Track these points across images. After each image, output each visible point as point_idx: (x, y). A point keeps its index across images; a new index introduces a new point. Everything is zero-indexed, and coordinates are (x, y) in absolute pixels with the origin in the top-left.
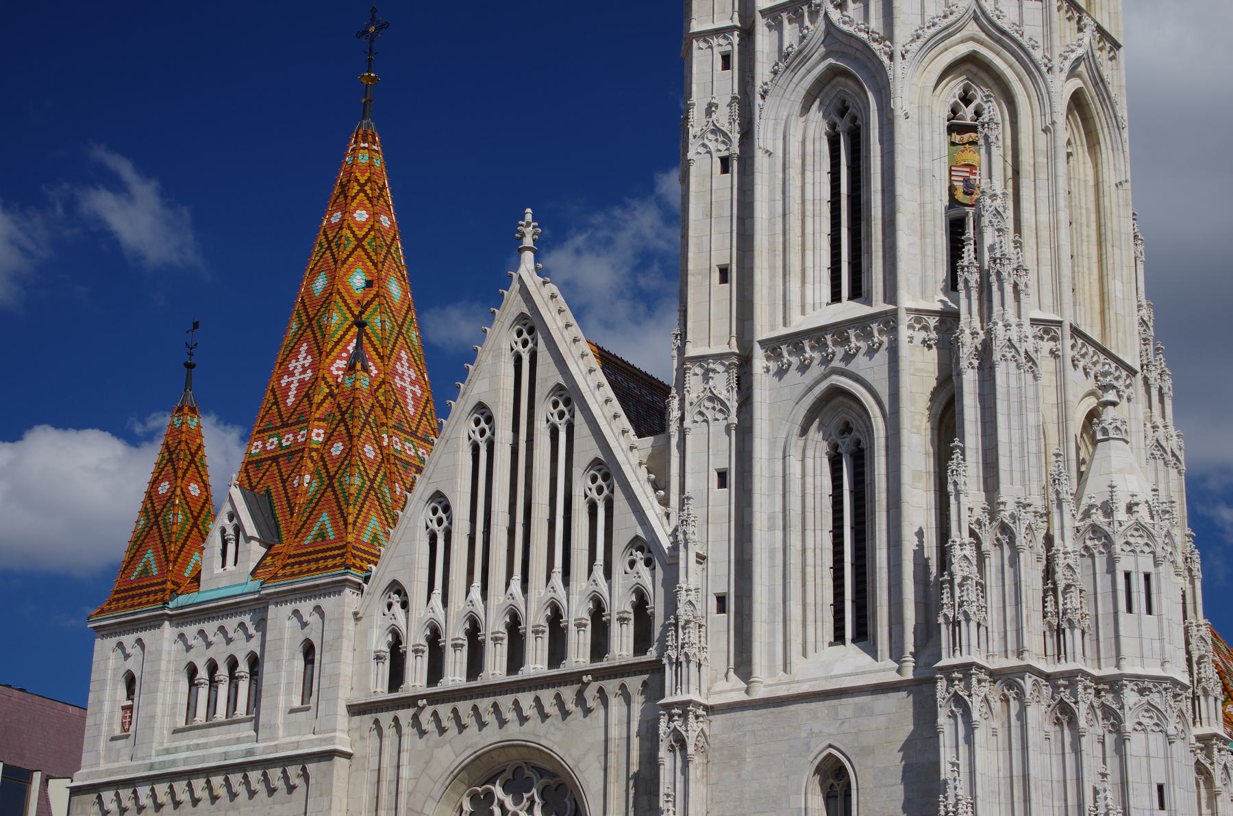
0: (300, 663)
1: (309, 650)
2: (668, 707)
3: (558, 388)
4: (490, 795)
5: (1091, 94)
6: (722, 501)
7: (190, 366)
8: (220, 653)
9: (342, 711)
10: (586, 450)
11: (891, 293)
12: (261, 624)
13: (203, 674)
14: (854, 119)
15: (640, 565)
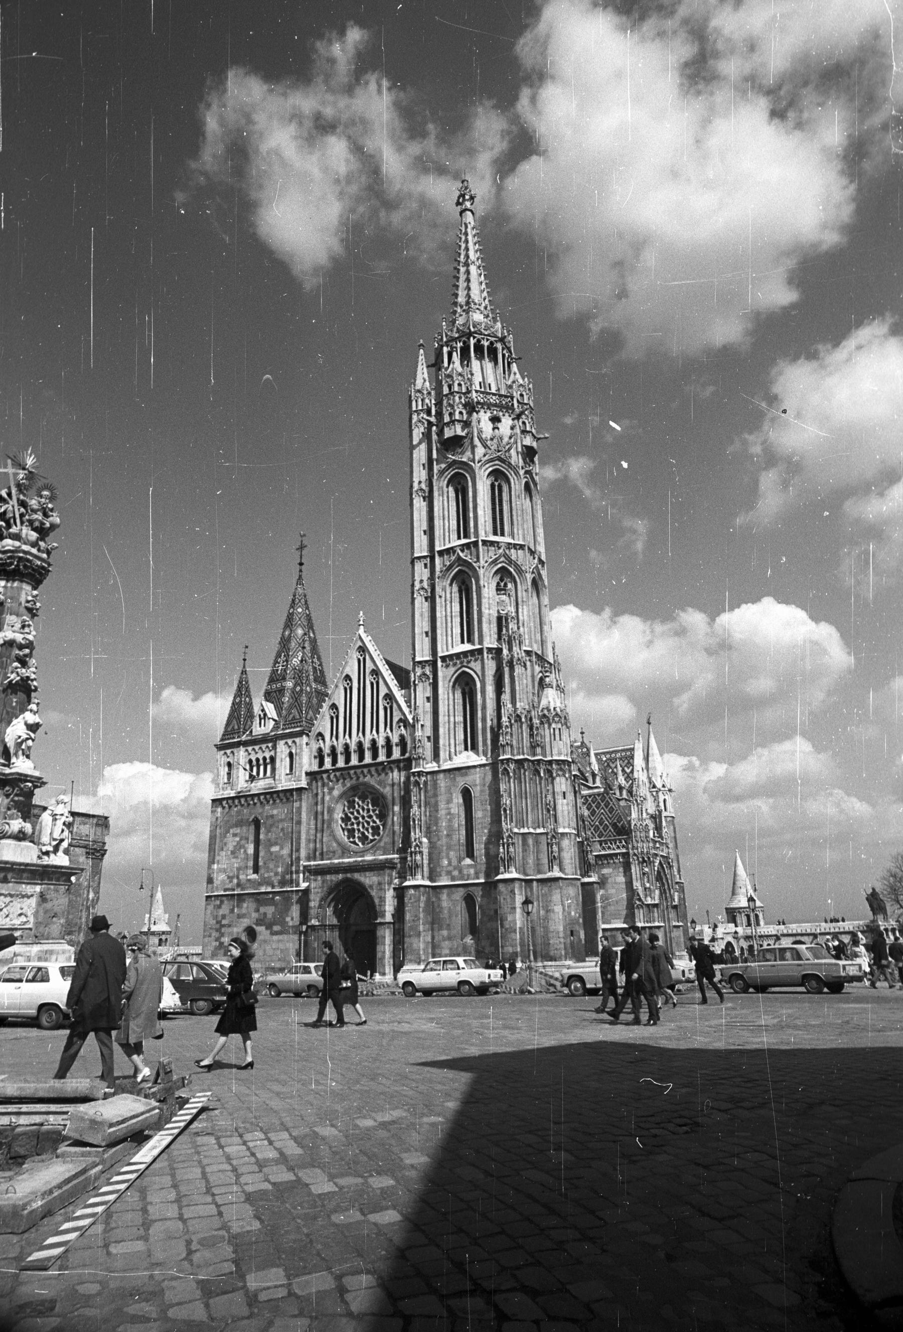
0: (288, 759)
1: (291, 755)
2: (414, 773)
3: (373, 670)
4: (354, 801)
5: (537, 578)
6: (428, 706)
7: (245, 660)
8: (260, 756)
9: (304, 775)
10: (383, 691)
11: (481, 642)
12: (274, 747)
13: (254, 763)
14: (467, 585)
15: (402, 728)
